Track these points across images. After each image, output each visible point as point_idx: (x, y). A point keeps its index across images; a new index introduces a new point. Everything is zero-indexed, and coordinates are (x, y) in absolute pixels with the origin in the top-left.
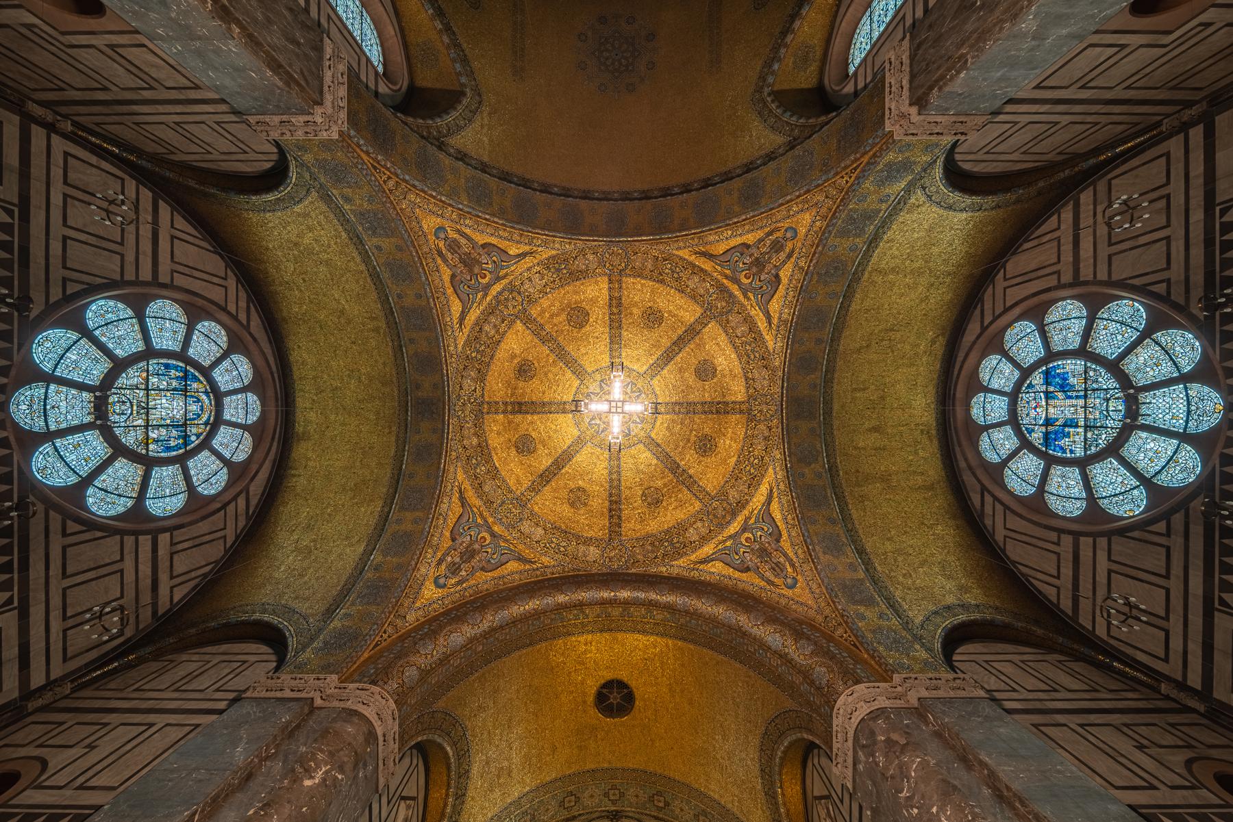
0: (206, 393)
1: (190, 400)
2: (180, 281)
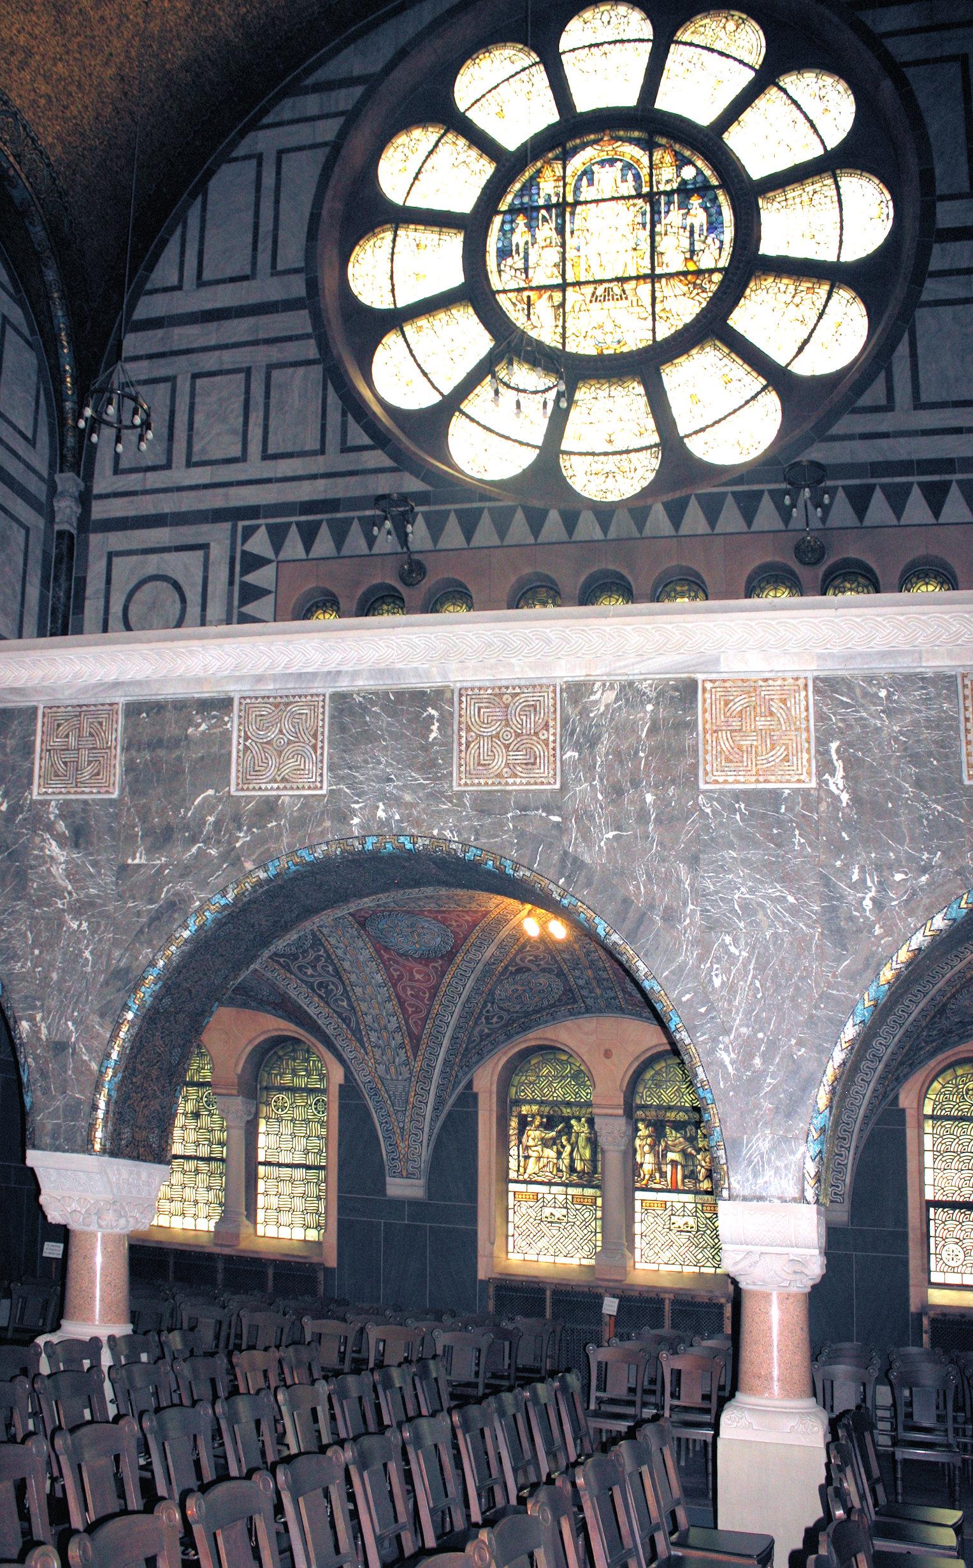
0: (565, 157)
1: (587, 193)
2: (292, 252)
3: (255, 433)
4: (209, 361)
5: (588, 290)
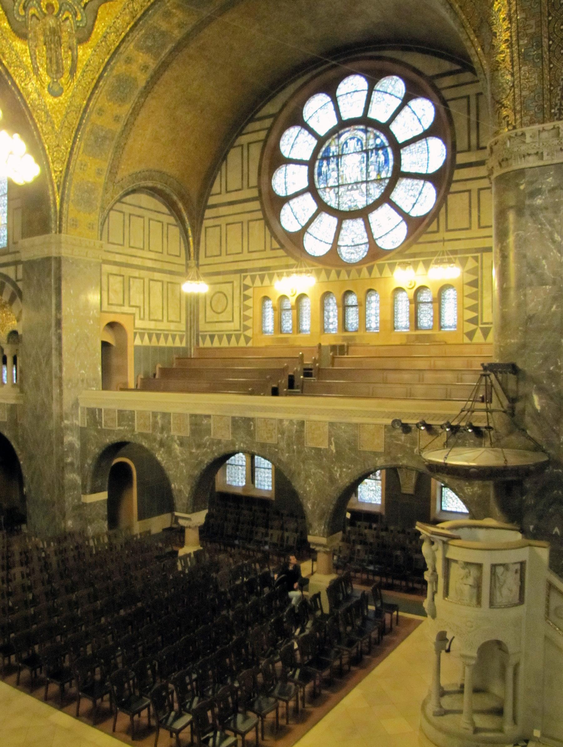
3: (245, 244)
4: (230, 219)
5: (346, 187)
